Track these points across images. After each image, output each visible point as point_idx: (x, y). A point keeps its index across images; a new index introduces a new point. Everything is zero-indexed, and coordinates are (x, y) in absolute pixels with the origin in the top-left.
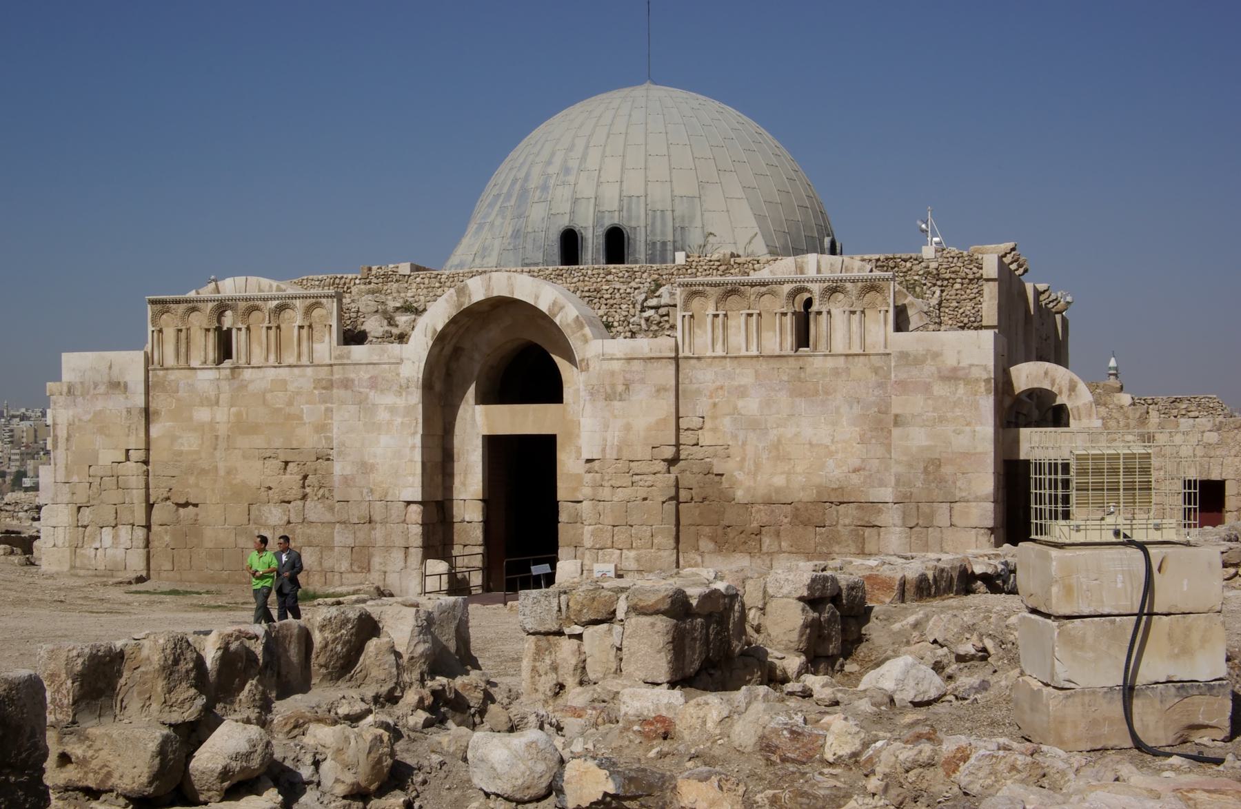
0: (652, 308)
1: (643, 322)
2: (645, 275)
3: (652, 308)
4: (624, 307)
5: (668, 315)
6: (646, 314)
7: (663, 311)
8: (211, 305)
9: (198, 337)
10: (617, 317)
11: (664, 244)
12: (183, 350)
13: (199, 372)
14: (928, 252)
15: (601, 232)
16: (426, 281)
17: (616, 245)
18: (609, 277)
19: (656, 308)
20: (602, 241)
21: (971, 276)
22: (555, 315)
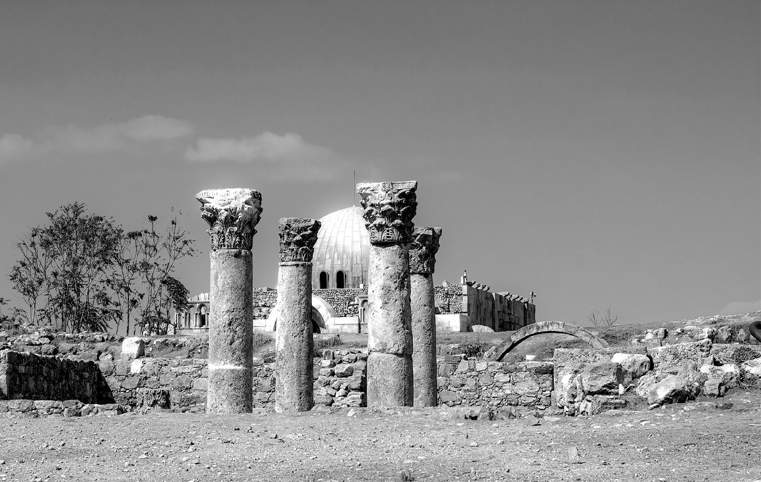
0: (351, 305)
1: (349, 310)
2: (349, 293)
3: (351, 305)
4: (342, 304)
5: (357, 308)
6: (349, 308)
7: (355, 306)
8: (198, 305)
9: (193, 317)
10: (340, 309)
11: (359, 277)
12: (188, 322)
13: (194, 330)
14: (445, 284)
15: (335, 272)
16: (273, 294)
17: (341, 278)
18: (337, 293)
19: (353, 305)
20: (335, 276)
21: (458, 294)
22: (318, 309)
